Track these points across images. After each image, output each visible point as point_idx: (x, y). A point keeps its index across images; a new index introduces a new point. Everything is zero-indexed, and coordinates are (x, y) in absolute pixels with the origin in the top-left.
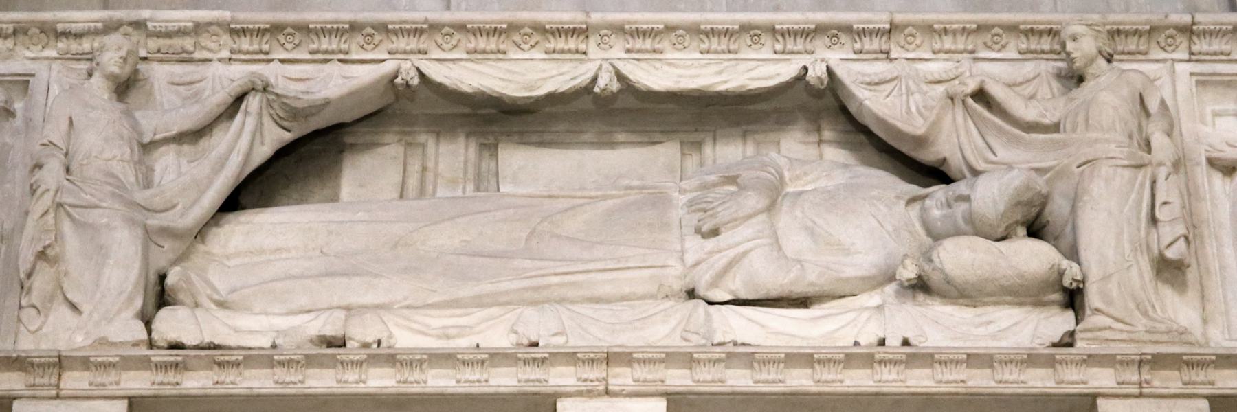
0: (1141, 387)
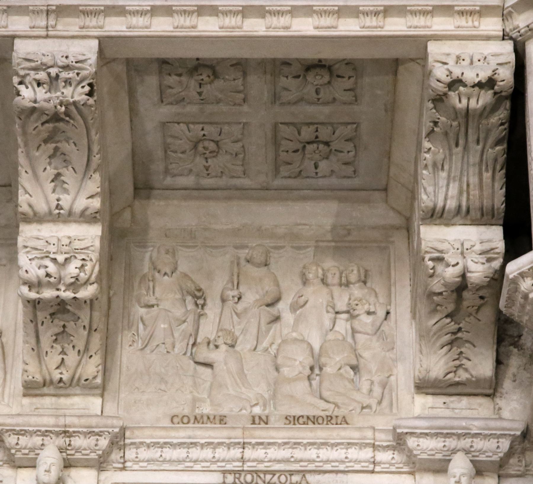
0: (48, 31)
